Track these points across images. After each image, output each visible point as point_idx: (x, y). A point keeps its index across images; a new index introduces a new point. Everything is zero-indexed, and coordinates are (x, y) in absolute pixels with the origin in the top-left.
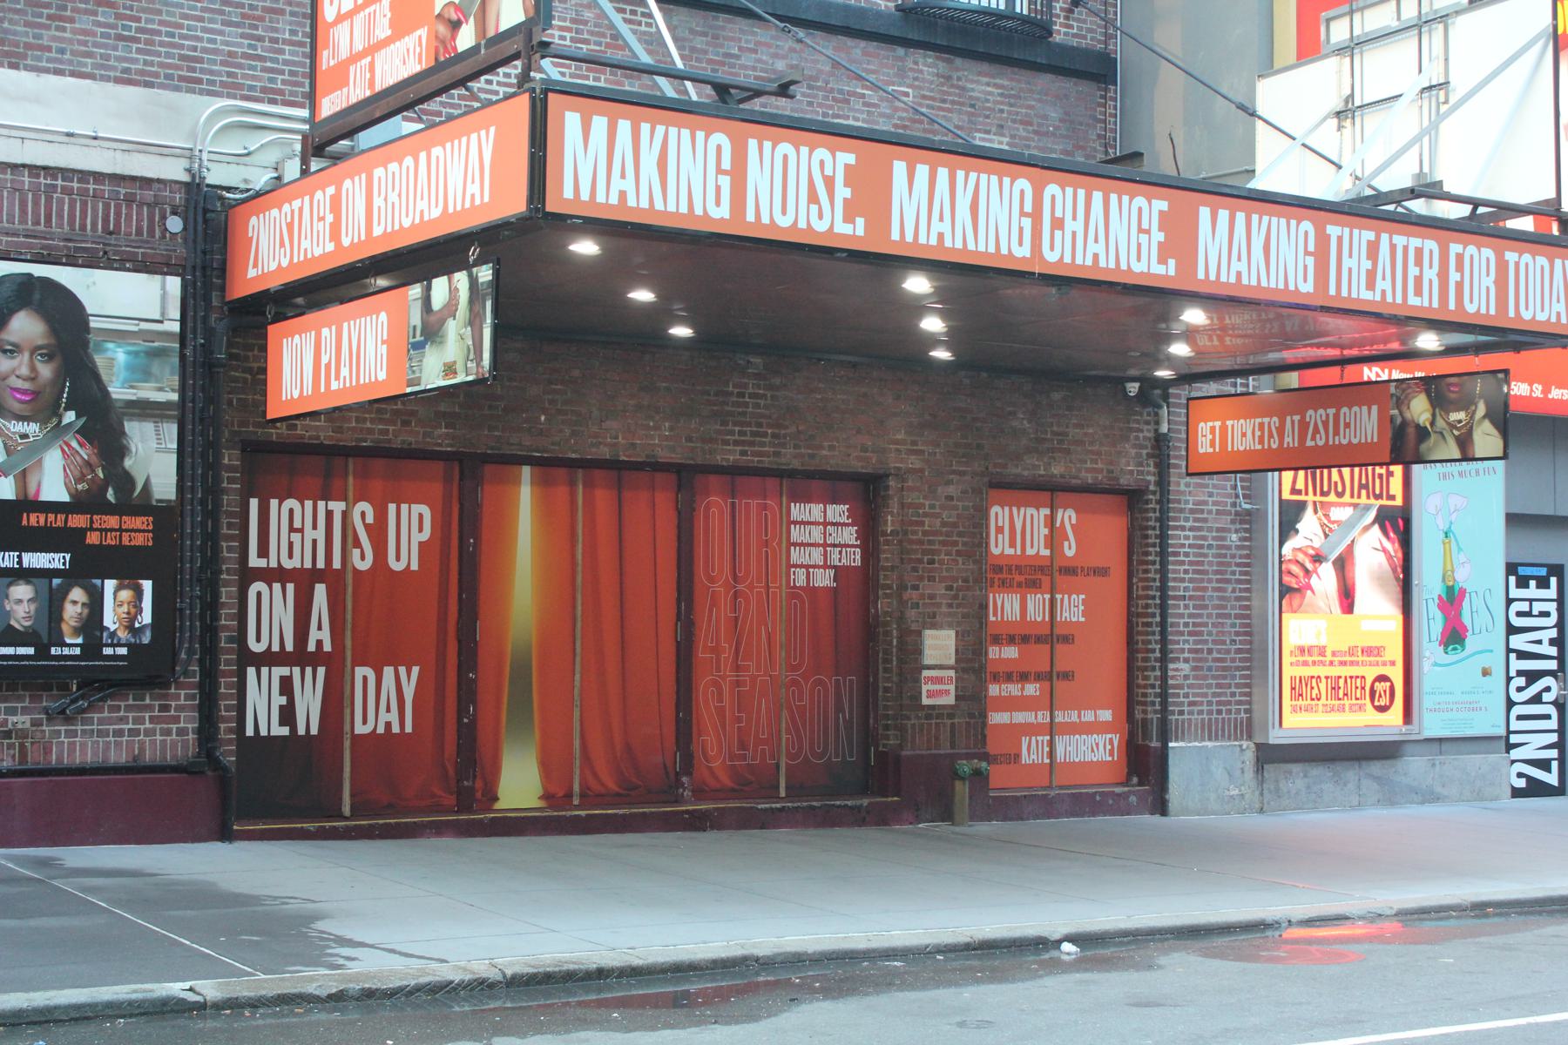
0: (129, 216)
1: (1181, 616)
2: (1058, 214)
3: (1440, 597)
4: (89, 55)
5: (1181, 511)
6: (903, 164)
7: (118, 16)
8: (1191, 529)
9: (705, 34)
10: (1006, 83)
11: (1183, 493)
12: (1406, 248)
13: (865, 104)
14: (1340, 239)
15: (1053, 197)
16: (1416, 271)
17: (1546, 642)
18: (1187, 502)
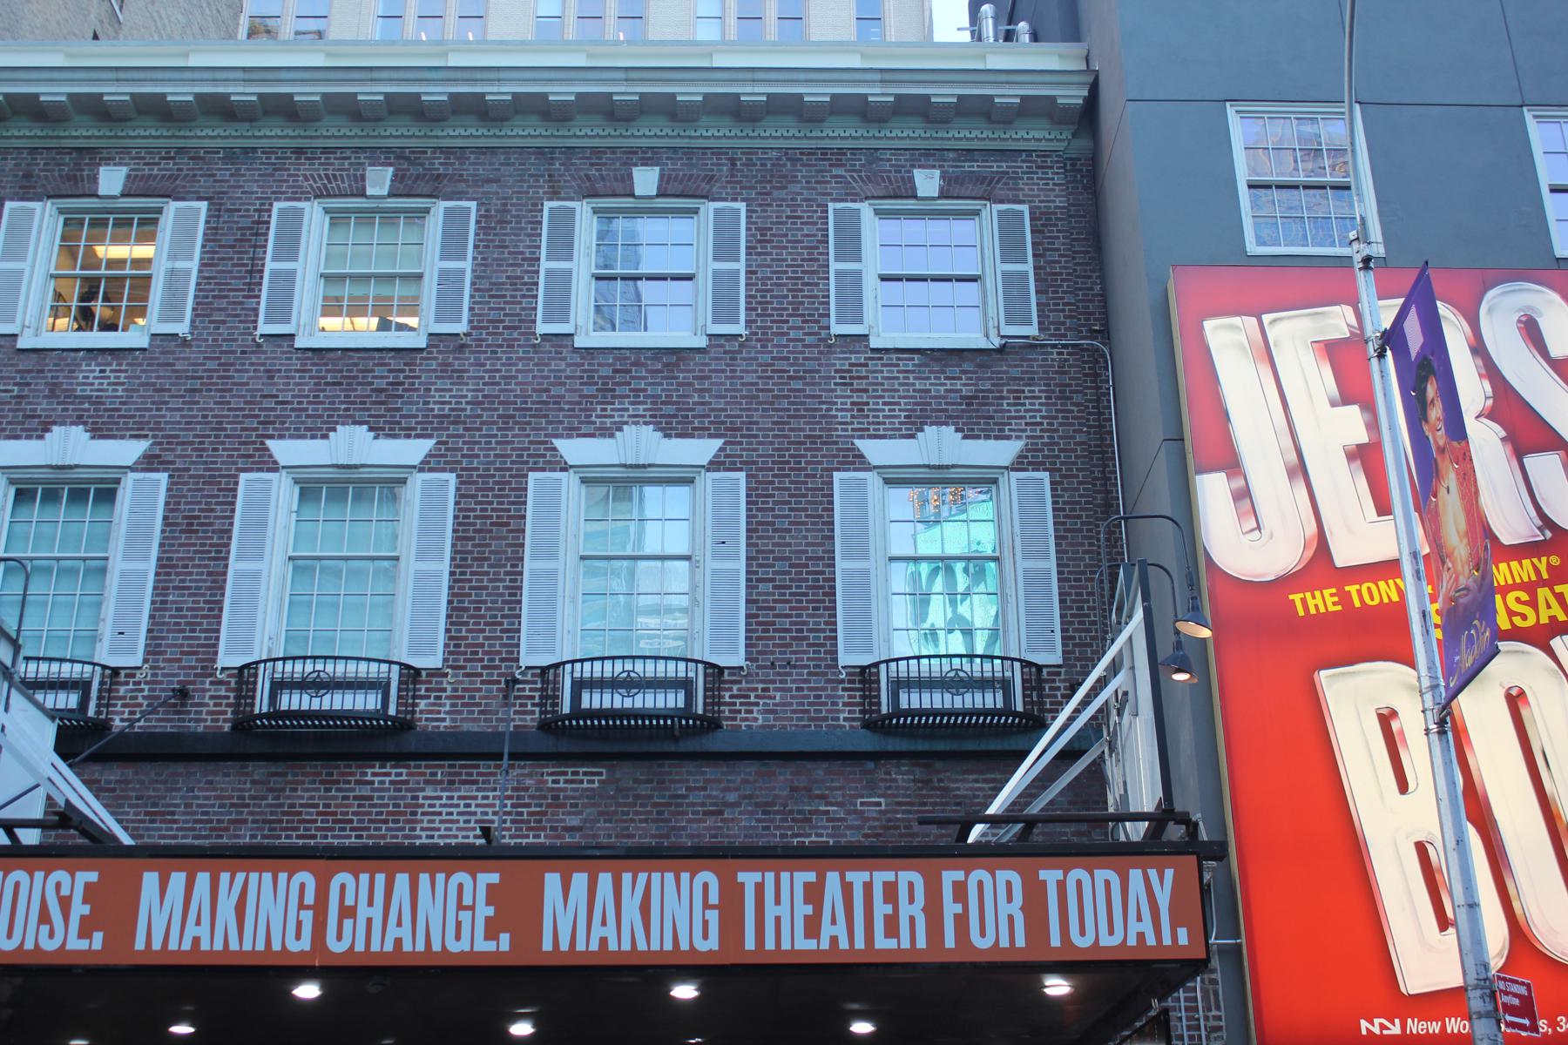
2: (349, 901)
6: (557, 876)
9: (650, 781)
12: (868, 887)
13: (829, 820)
14: (760, 888)
15: (343, 887)
16: (889, 909)
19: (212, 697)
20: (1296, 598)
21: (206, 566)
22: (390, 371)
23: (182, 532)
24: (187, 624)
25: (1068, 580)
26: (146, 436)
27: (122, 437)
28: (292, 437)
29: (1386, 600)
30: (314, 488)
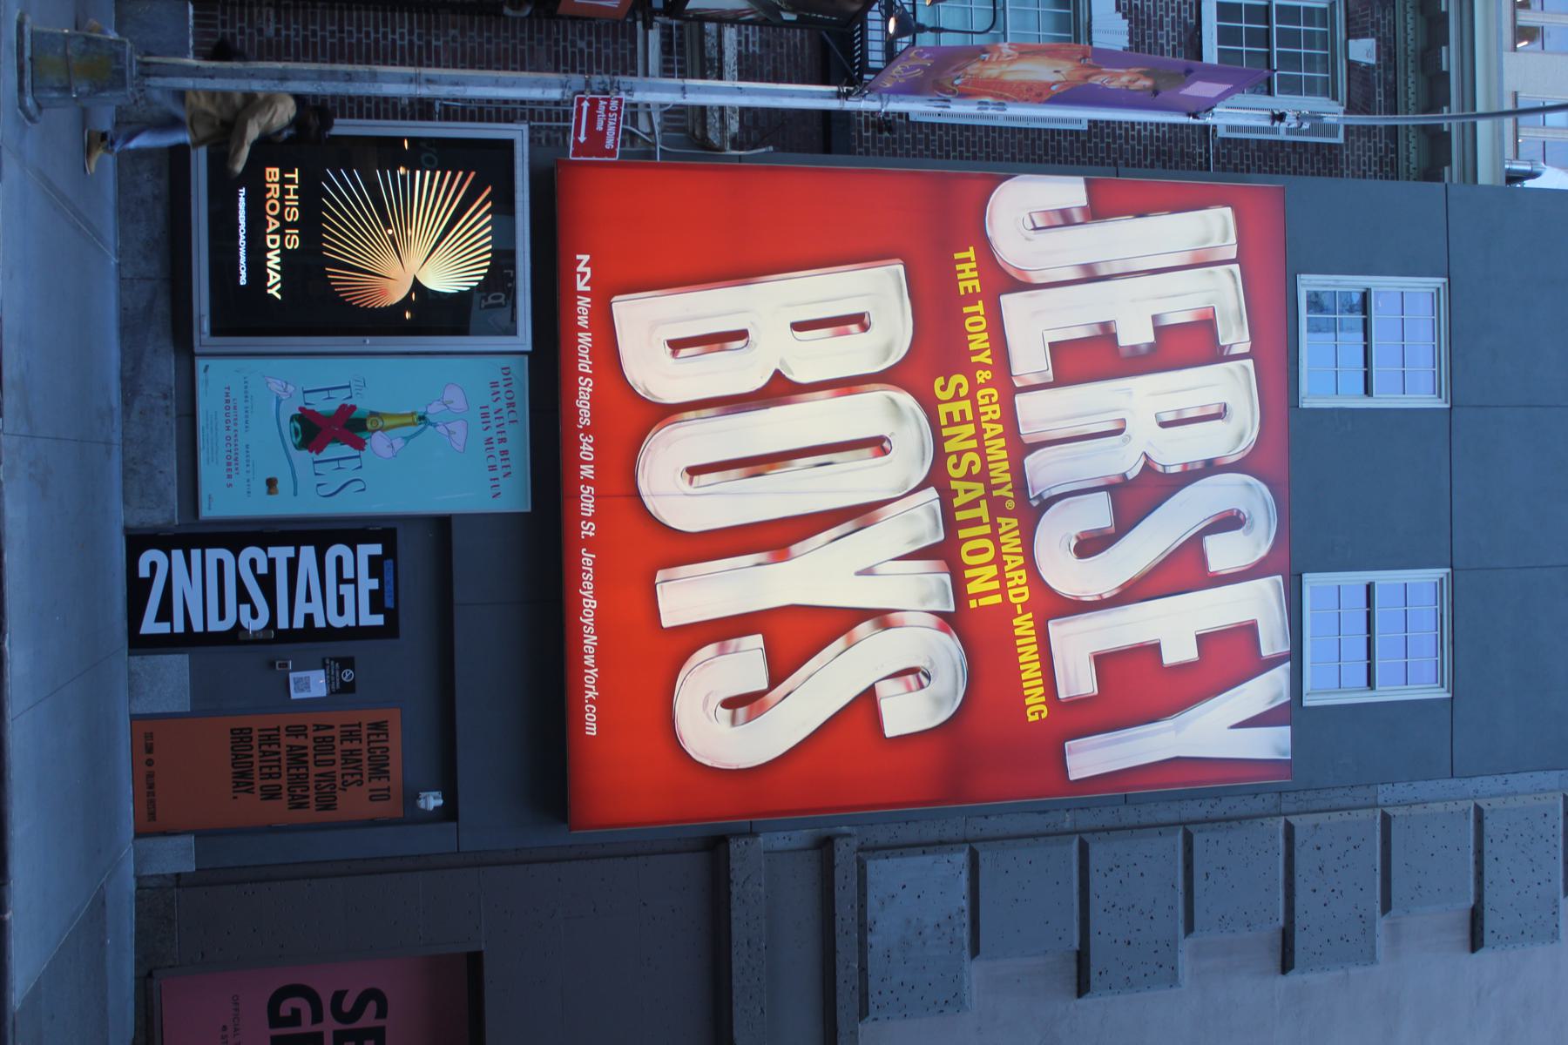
1: (323, 28)
3: (354, 408)
5: (428, 33)
8: (411, 43)
10: (807, 52)
11: (446, 34)
17: (309, 608)
18: (437, 39)
20: (971, 254)
25: (987, 136)
29: (970, 337)
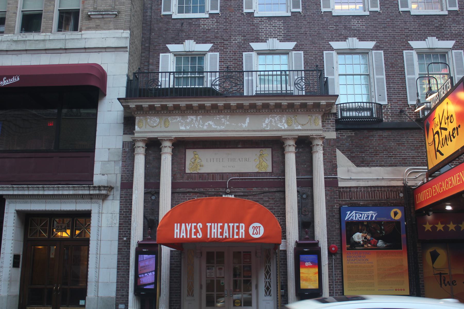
0: (391, 194)
4: (383, 161)
7: (388, 152)
19: (408, 113)
21: (399, 77)
22: (439, 21)
23: (390, 67)
24: (397, 93)
26: (374, 40)
27: (368, 41)
28: (415, 40)
30: (421, 54)
